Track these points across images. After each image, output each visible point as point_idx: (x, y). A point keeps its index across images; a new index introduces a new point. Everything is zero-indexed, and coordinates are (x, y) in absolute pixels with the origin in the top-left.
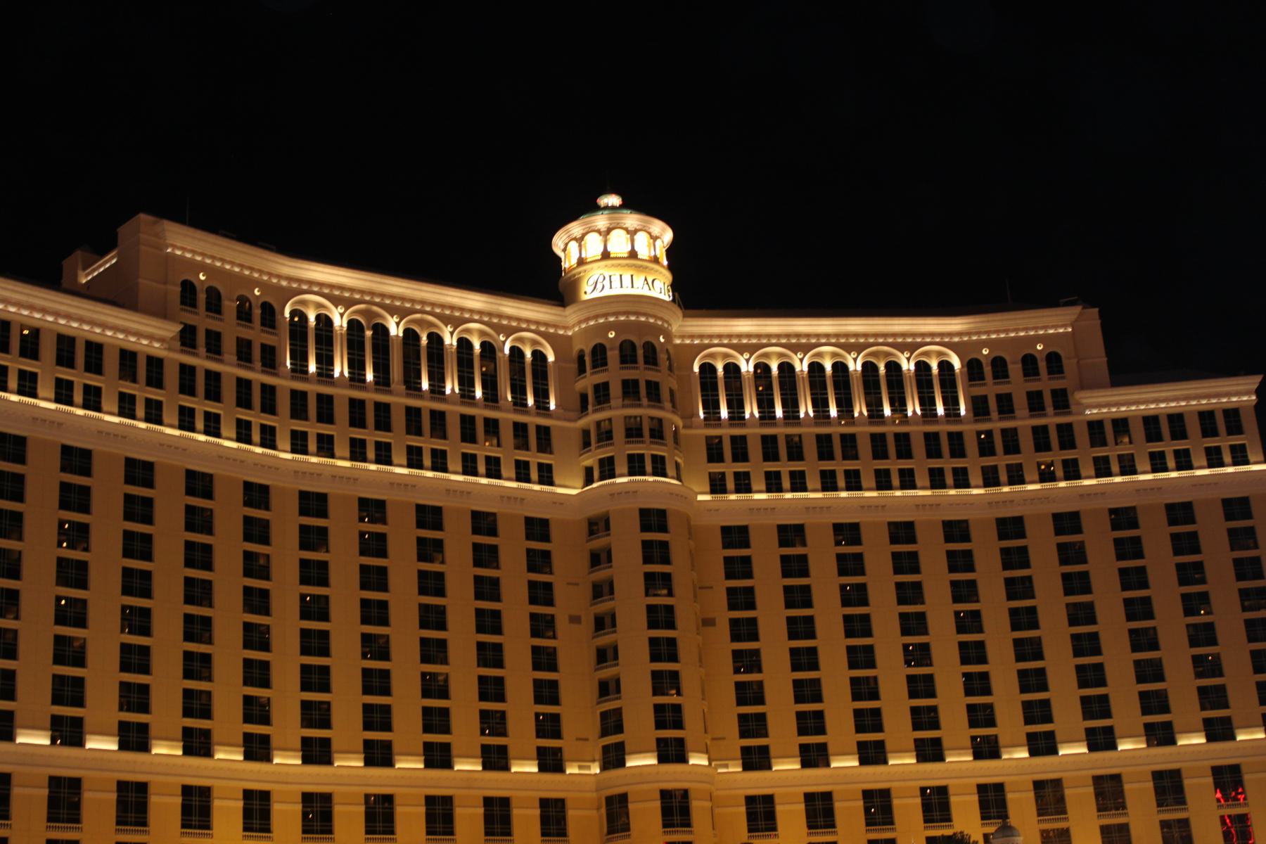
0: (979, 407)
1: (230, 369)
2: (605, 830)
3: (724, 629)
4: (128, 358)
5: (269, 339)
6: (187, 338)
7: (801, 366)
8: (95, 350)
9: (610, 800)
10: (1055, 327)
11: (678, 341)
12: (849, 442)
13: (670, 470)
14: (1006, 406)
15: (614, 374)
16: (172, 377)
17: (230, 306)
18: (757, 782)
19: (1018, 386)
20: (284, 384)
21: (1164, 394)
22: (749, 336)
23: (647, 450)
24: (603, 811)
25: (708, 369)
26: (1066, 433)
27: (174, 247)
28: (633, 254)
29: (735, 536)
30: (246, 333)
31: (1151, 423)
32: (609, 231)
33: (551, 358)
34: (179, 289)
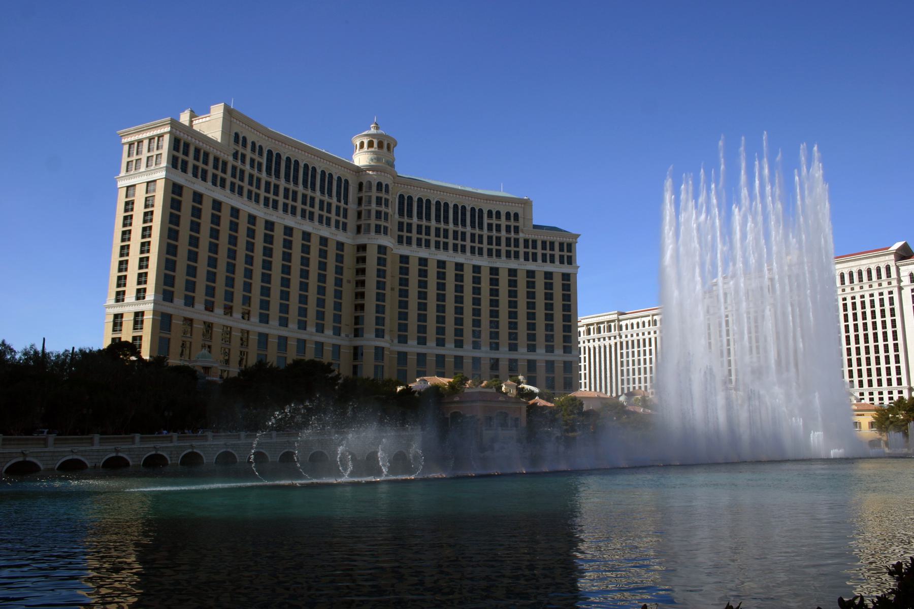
0: (490, 226)
2: (352, 359)
3: (397, 293)
4: (216, 159)
5: (261, 160)
6: (235, 156)
9: (356, 348)
14: (498, 228)
15: (374, 194)
18: (402, 348)
19: (503, 222)
23: (382, 223)
24: (352, 351)
25: (401, 197)
29: (404, 259)
30: (254, 157)
31: (544, 243)
33: (350, 182)
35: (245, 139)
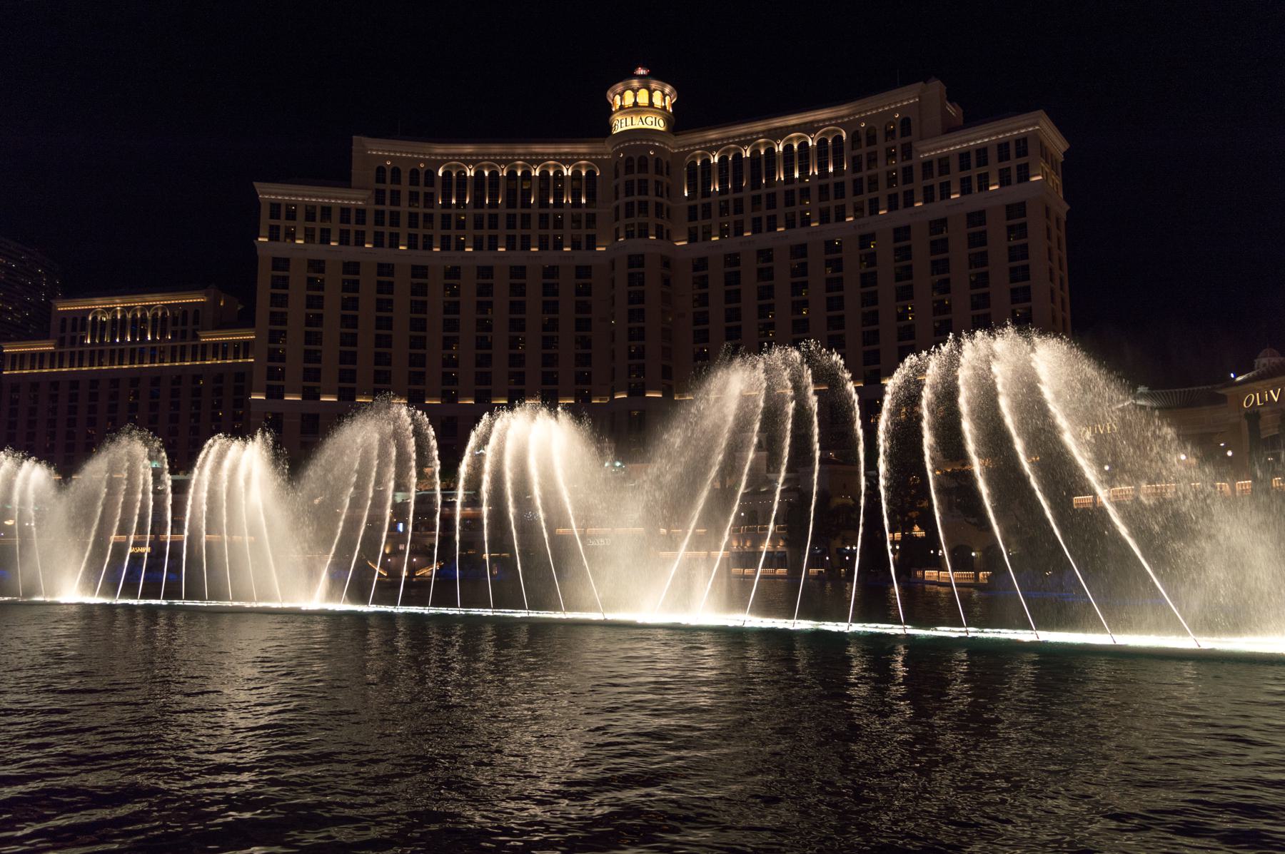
1: (404, 208)
6: (379, 197)
7: (747, 153)
8: (327, 211)
10: (908, 100)
11: (676, 151)
12: (805, 192)
13: (652, 230)
16: (370, 218)
17: (405, 177)
20: (437, 212)
21: (973, 136)
22: (716, 140)
26: (908, 173)
27: (372, 150)
28: (636, 104)
32: (624, 91)
34: (375, 171)
35: (396, 172)
